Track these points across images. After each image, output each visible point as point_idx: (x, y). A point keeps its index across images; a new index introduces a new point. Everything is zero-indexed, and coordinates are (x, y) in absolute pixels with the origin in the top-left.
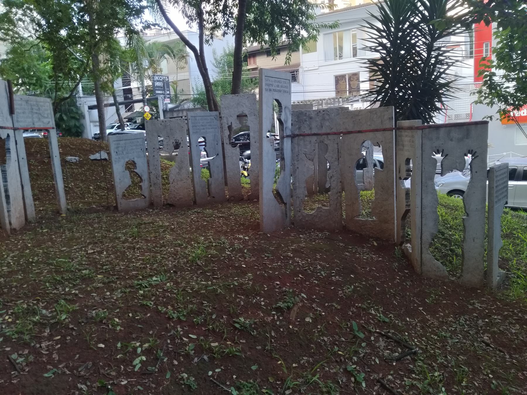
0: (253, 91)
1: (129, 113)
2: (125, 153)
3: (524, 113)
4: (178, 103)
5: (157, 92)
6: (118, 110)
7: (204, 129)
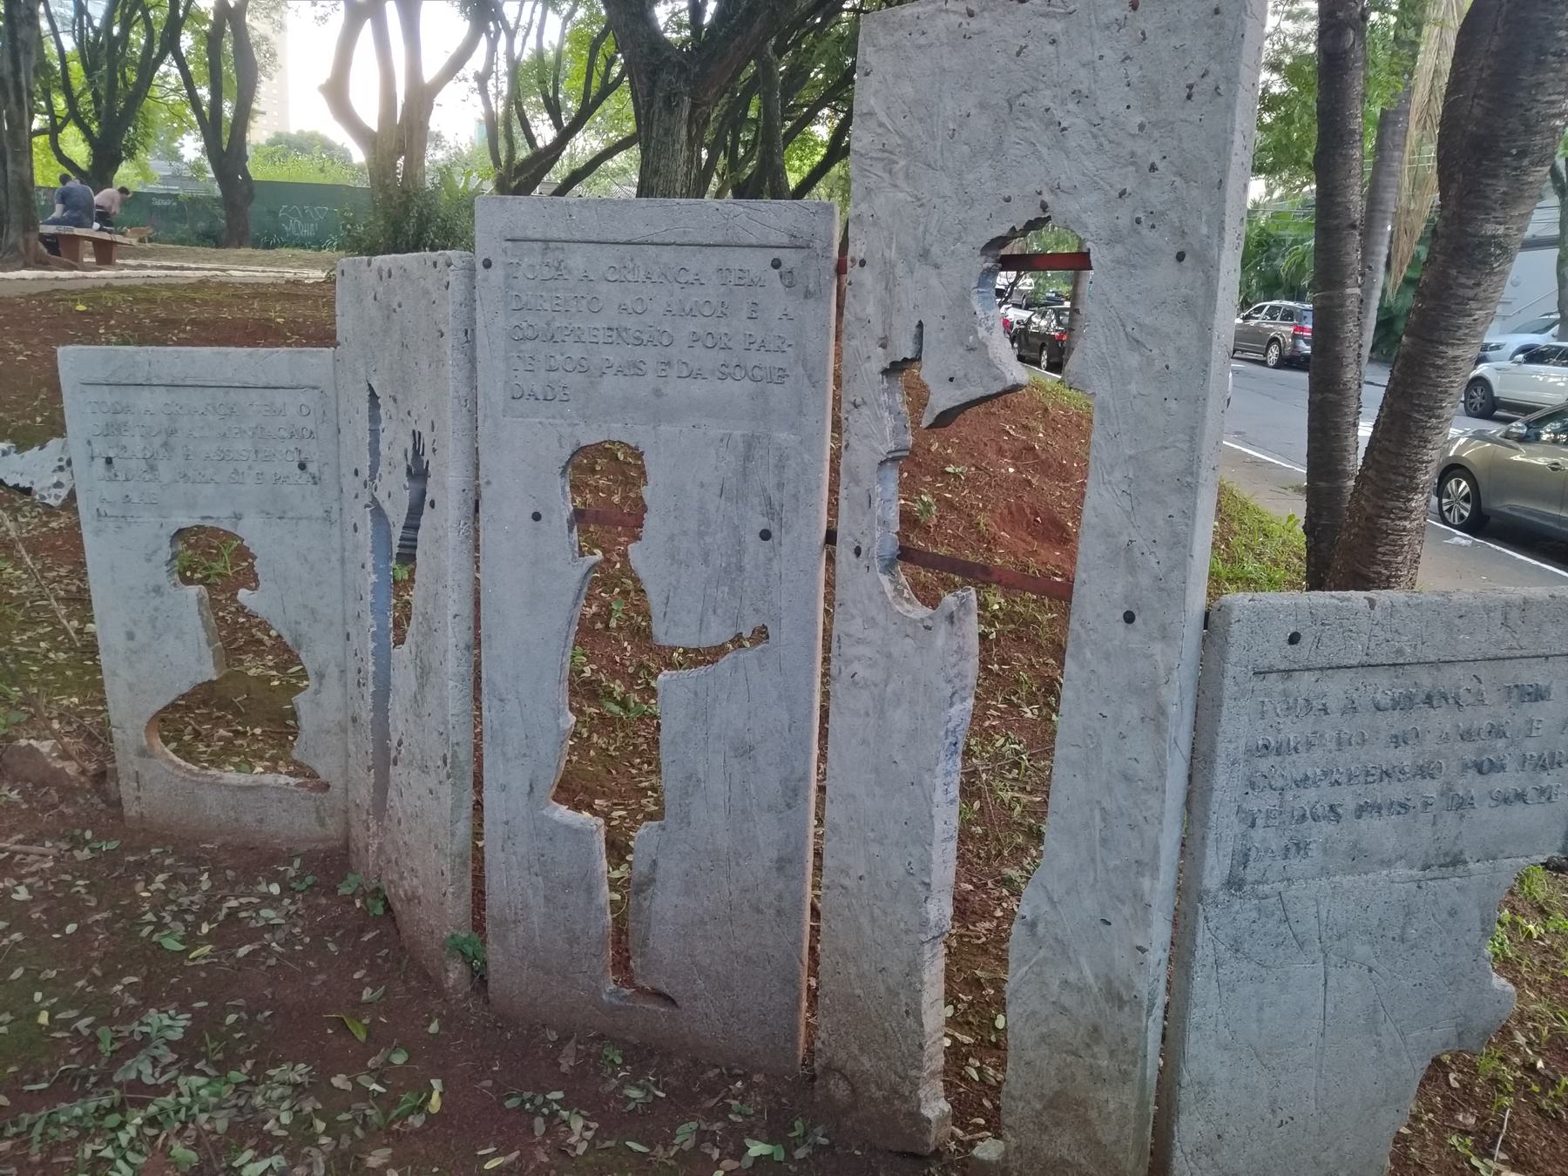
2: (165, 471)
7: (636, 369)
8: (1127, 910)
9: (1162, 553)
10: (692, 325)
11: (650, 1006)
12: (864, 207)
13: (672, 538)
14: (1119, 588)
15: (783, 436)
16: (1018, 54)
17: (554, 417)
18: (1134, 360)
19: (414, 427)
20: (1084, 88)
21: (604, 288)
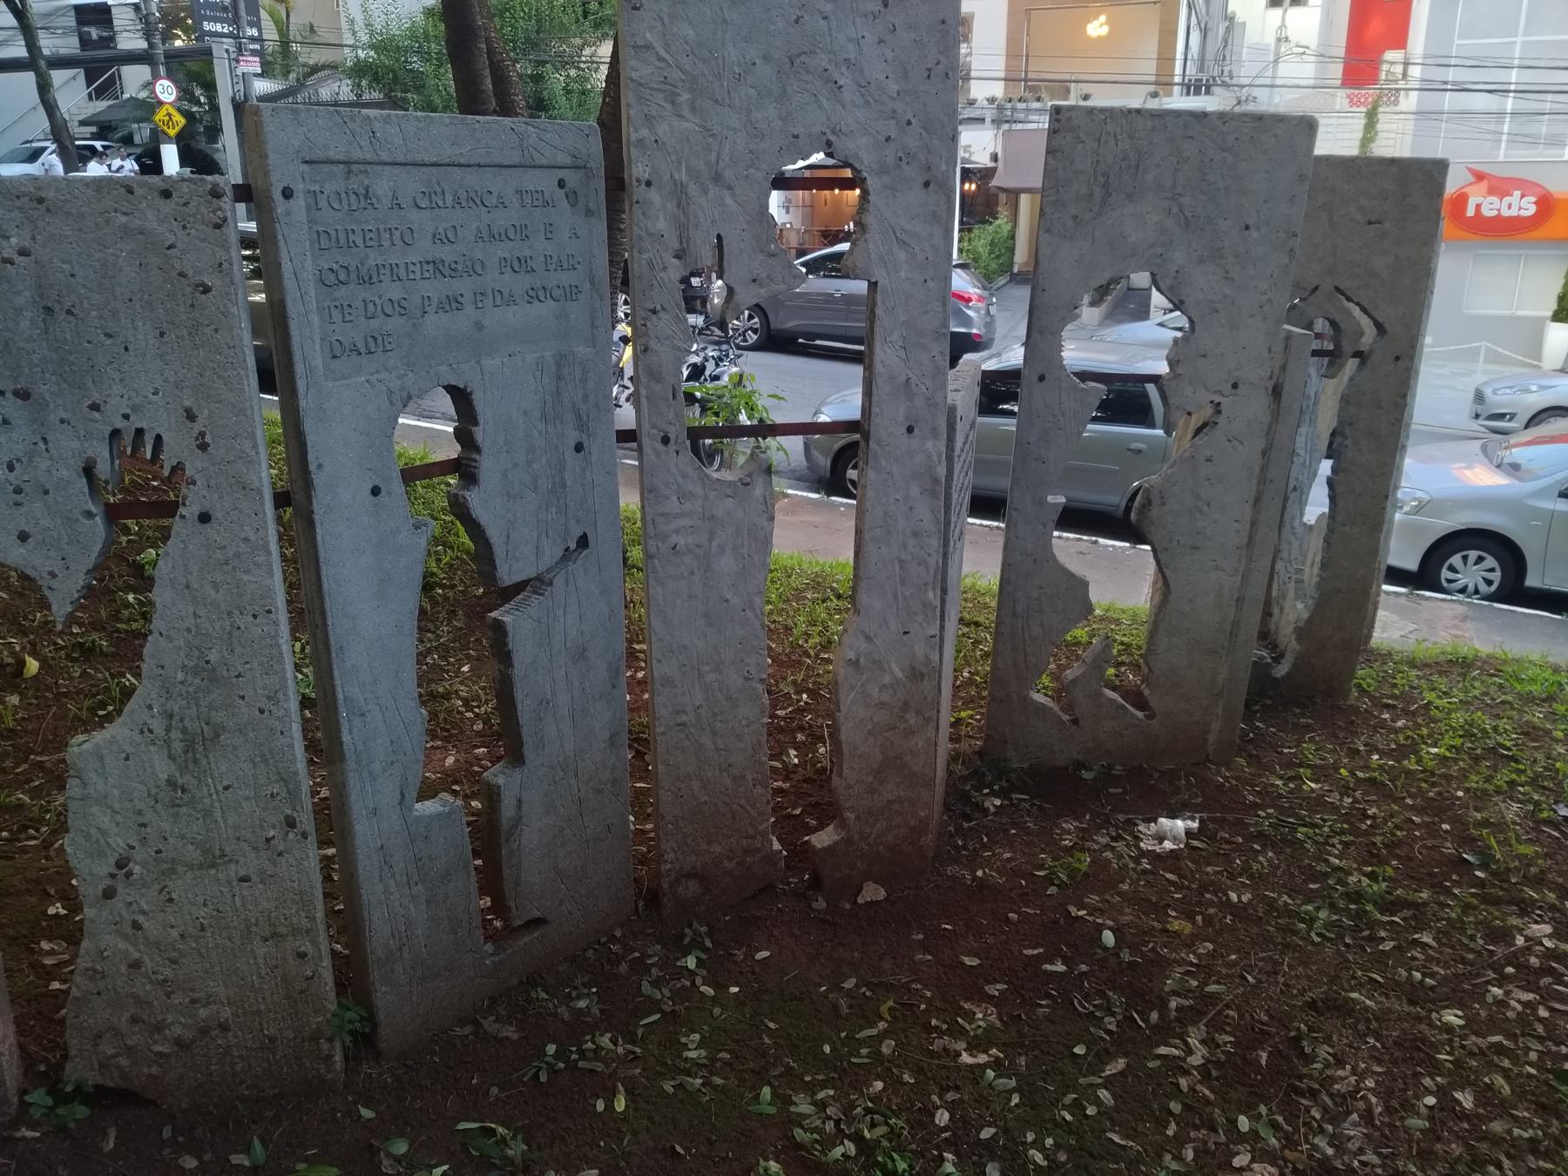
0: (587, 51)
1: (101, 105)
3: (1510, 206)
4: (292, 76)
5: (207, 26)
6: (44, 88)
7: (453, 303)
8: (919, 618)
9: (929, 383)
10: (502, 250)
11: (527, 939)
12: (645, 132)
13: (505, 475)
14: (902, 412)
15: (582, 350)
16: (797, 21)
17: (378, 372)
18: (901, 255)
19: (119, 423)
20: (852, 57)
21: (414, 216)
